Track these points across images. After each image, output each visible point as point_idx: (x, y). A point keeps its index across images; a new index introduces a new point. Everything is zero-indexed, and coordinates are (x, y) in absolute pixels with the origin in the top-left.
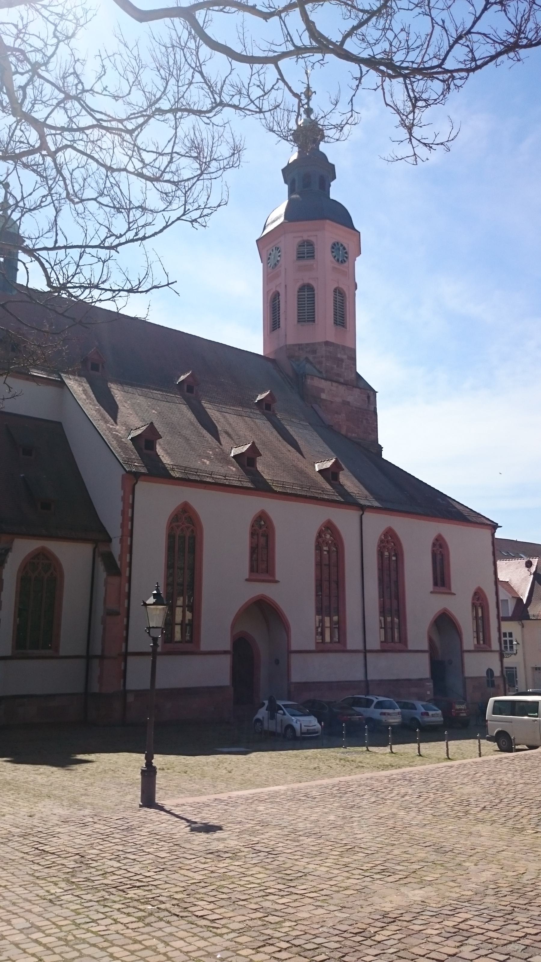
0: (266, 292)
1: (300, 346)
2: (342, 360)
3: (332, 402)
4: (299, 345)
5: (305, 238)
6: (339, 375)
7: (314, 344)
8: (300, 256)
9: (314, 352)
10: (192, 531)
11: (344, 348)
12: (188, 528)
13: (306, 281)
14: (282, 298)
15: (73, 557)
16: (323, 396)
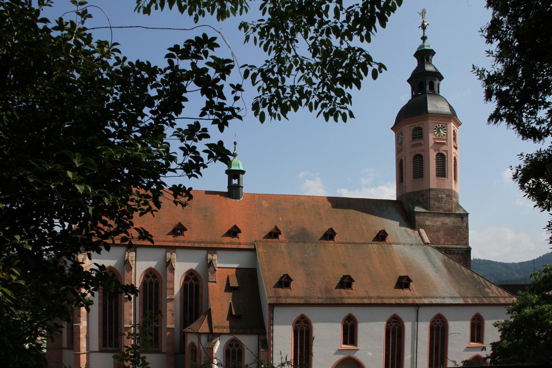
0: (397, 159)
1: (414, 193)
2: (442, 198)
3: (433, 226)
4: (413, 192)
5: (417, 126)
6: (439, 208)
7: (422, 191)
8: (414, 137)
9: (423, 196)
10: (308, 327)
11: (443, 190)
12: (305, 326)
13: (417, 153)
14: (404, 163)
15: (249, 342)
16: (428, 223)
